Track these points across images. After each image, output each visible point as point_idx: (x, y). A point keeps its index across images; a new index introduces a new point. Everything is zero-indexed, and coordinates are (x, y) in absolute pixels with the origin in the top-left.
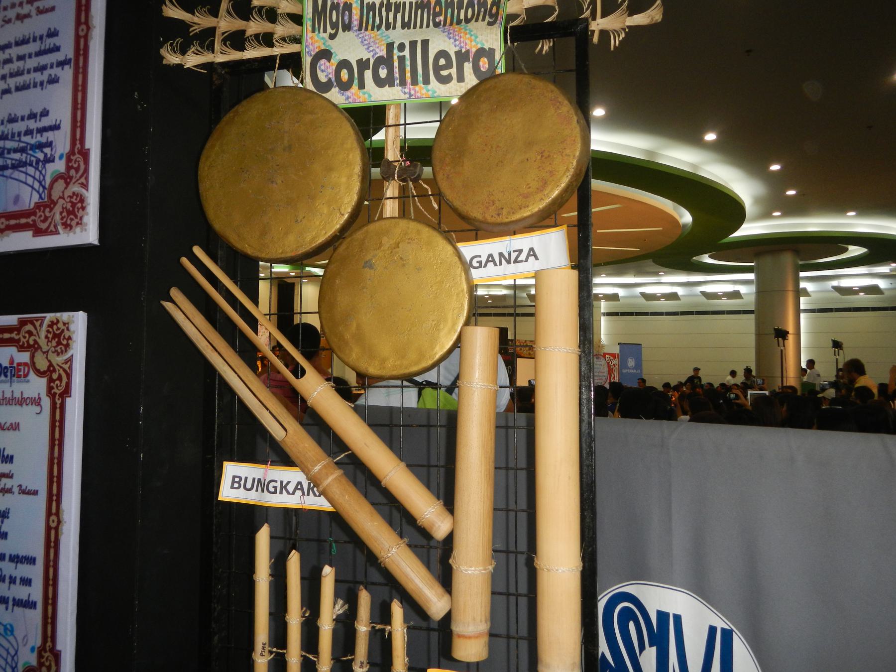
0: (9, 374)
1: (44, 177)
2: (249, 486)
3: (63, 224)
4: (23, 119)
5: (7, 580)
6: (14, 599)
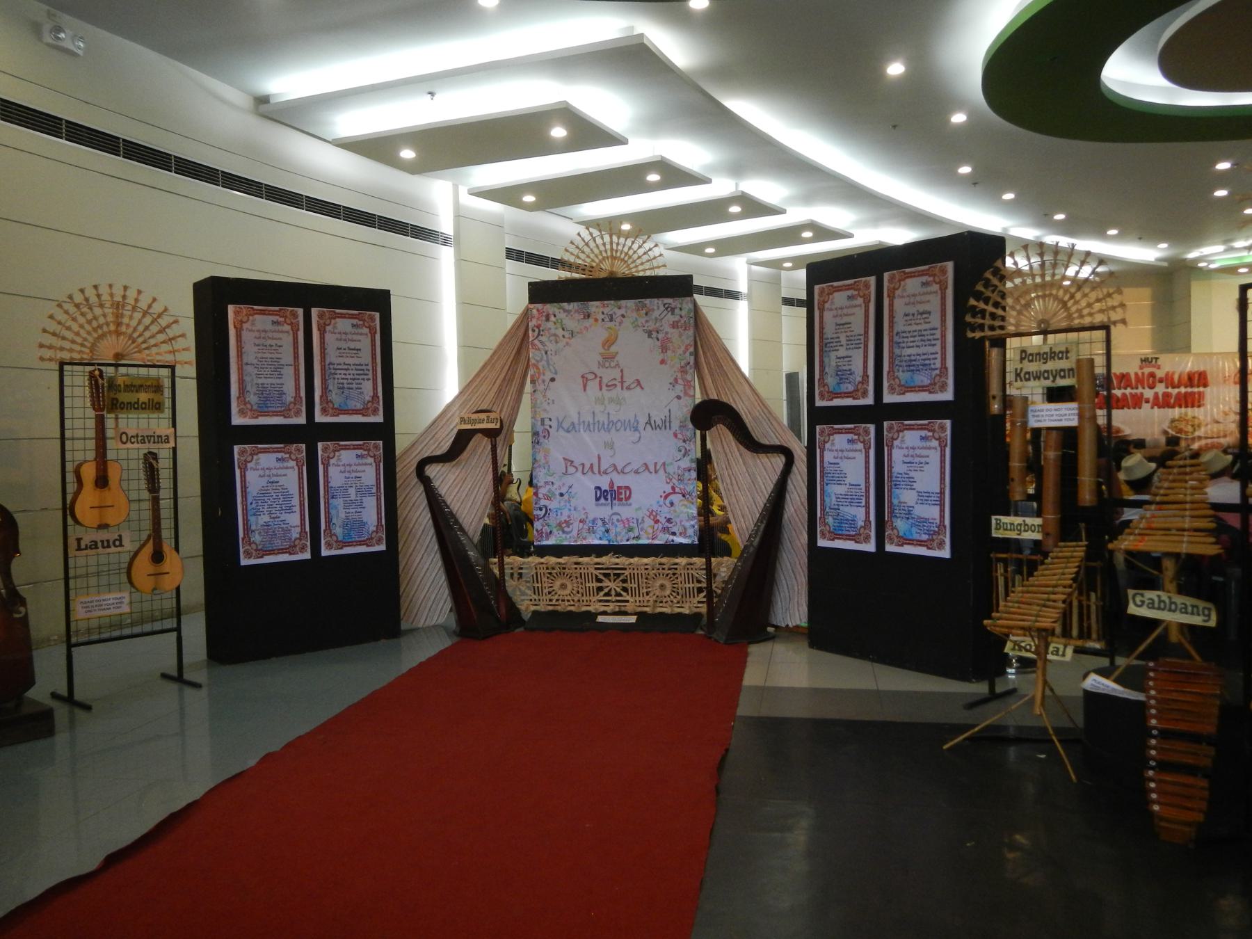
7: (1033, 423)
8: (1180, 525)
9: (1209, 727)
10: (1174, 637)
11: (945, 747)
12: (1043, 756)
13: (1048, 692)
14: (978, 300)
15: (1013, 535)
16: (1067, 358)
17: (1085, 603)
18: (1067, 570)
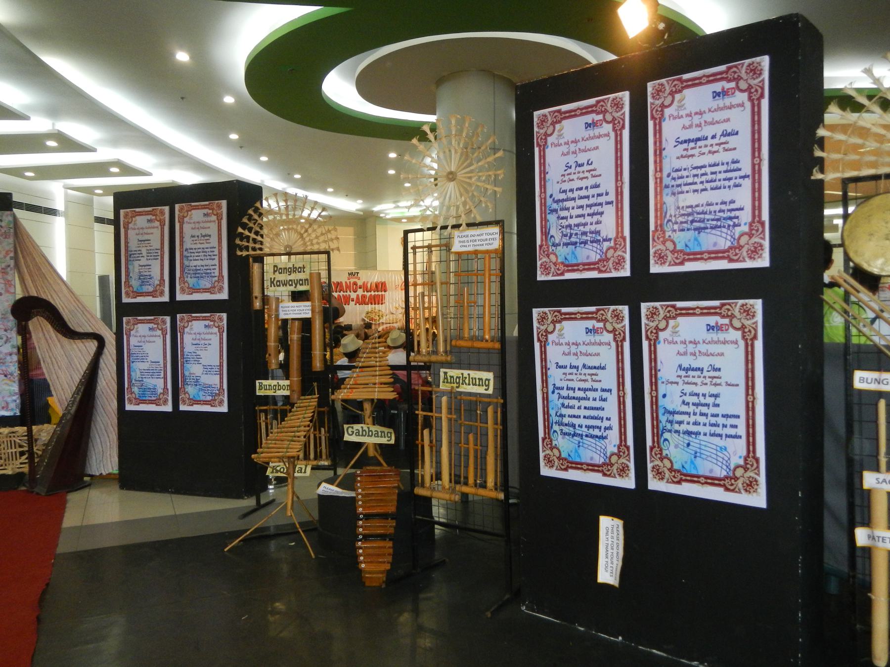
0: (715, 329)
1: (734, 234)
2: (869, 381)
3: (749, 257)
4: (717, 204)
5: (721, 426)
6: (726, 435)
7: (282, 316)
8: (373, 381)
9: (392, 508)
10: (371, 453)
11: (226, 550)
12: (293, 544)
13: (295, 499)
14: (244, 229)
15: (270, 393)
16: (304, 272)
17: (318, 436)
18: (306, 415)
